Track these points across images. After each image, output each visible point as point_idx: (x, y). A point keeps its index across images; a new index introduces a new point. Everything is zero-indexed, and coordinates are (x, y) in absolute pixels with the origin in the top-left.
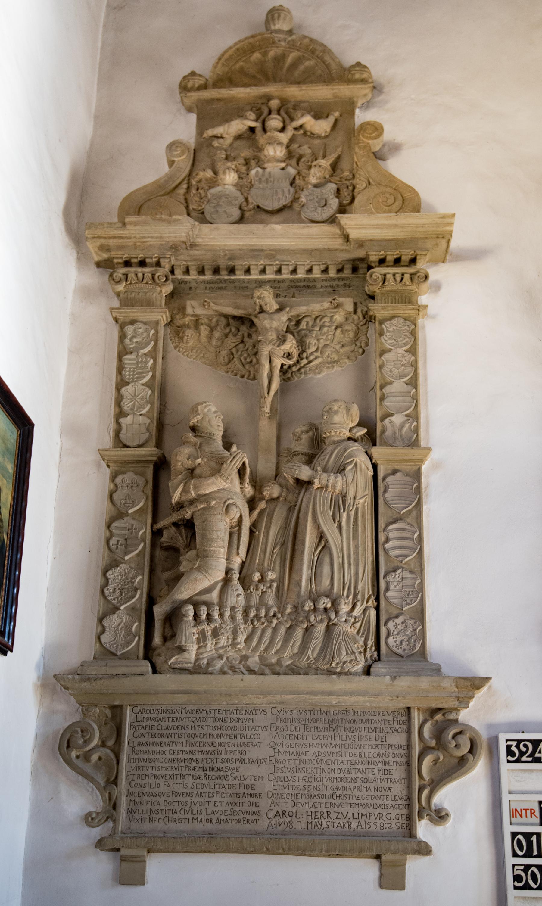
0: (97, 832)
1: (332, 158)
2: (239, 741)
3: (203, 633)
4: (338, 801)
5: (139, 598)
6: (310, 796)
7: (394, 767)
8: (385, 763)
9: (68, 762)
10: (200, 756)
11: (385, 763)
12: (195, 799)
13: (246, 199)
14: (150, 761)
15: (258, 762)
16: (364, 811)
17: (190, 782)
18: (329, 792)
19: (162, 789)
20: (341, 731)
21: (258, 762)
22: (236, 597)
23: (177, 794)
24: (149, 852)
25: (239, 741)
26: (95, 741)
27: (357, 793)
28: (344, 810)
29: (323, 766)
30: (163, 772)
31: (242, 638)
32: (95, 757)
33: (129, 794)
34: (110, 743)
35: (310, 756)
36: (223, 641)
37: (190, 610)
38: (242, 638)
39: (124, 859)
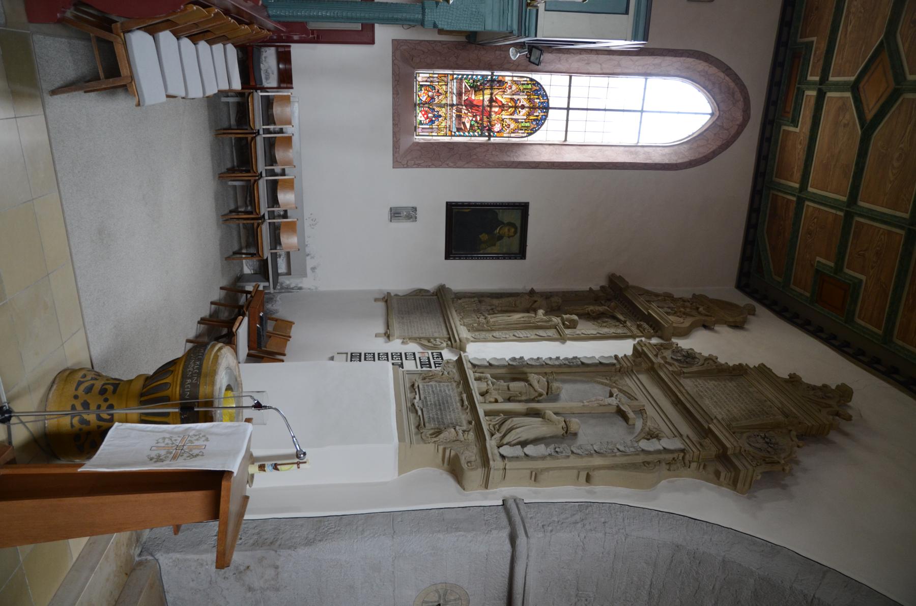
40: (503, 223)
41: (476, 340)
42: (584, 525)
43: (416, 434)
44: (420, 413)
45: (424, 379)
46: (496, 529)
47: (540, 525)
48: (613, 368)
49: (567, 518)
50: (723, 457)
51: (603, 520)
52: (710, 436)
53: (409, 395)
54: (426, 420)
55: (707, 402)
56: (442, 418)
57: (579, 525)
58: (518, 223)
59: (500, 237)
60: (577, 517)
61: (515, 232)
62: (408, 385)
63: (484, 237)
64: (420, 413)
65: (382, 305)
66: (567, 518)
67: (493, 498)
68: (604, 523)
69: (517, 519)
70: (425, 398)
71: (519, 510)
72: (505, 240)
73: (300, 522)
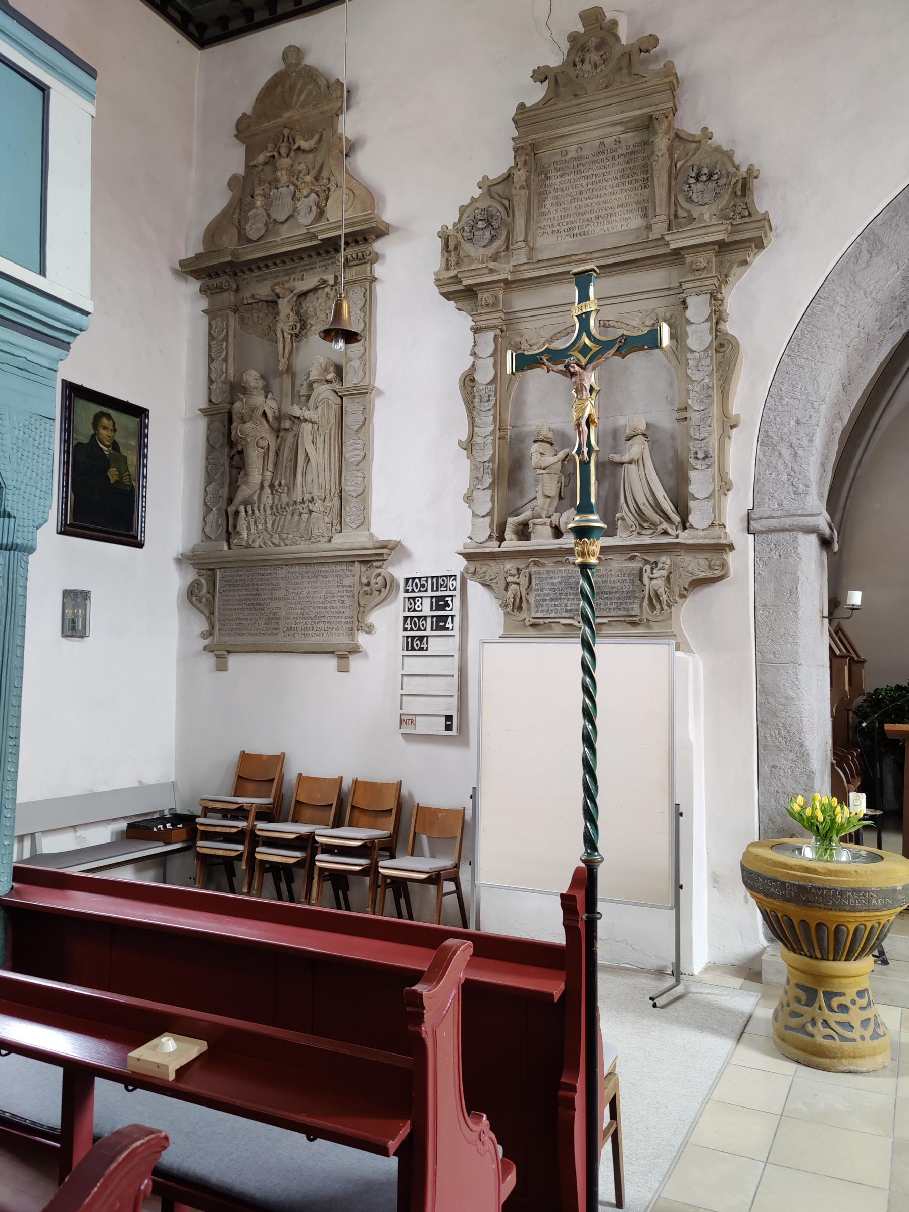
0: (207, 642)
1: (313, 172)
2: (270, 587)
3: (249, 523)
4: (318, 620)
5: (223, 502)
6: (304, 618)
7: (346, 598)
8: (342, 597)
9: (192, 603)
10: (252, 597)
11: (342, 597)
12: (250, 622)
13: (268, 215)
14: (228, 600)
15: (279, 599)
16: (329, 626)
17: (247, 612)
18: (312, 616)
19: (234, 617)
20: (320, 578)
21: (279, 599)
22: (267, 498)
23: (241, 620)
24: (229, 652)
25: (270, 587)
26: (204, 590)
27: (327, 615)
28: (321, 625)
29: (311, 600)
30: (235, 607)
31: (269, 525)
32: (204, 600)
33: (220, 620)
34: (211, 591)
35: (304, 594)
36: (260, 526)
37: (242, 508)
38: (269, 525)
39: (217, 656)
40: (93, 437)
41: (364, 523)
42: (801, 446)
43: (649, 627)
44: (605, 620)
45: (520, 608)
46: (795, 549)
47: (793, 496)
48: (500, 340)
49: (786, 466)
50: (722, 247)
51: (792, 423)
52: (682, 253)
53: (557, 630)
54: (624, 613)
55: (597, 229)
56: (618, 592)
57: (800, 452)
58: (97, 409)
59: (115, 445)
60: (786, 453)
61: (108, 417)
62: (532, 631)
63: (113, 474)
64: (605, 620)
65: (233, 661)
66: (786, 466)
67: (746, 545)
68: (798, 422)
69: (788, 522)
70: (567, 611)
71: (773, 517)
72: (118, 438)
73: (766, 769)
